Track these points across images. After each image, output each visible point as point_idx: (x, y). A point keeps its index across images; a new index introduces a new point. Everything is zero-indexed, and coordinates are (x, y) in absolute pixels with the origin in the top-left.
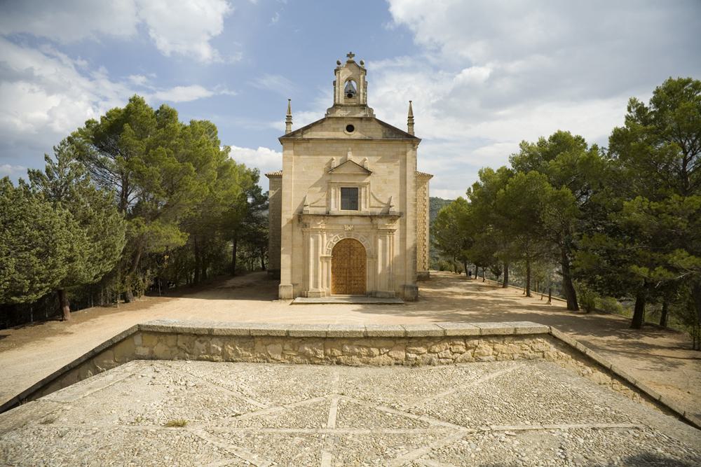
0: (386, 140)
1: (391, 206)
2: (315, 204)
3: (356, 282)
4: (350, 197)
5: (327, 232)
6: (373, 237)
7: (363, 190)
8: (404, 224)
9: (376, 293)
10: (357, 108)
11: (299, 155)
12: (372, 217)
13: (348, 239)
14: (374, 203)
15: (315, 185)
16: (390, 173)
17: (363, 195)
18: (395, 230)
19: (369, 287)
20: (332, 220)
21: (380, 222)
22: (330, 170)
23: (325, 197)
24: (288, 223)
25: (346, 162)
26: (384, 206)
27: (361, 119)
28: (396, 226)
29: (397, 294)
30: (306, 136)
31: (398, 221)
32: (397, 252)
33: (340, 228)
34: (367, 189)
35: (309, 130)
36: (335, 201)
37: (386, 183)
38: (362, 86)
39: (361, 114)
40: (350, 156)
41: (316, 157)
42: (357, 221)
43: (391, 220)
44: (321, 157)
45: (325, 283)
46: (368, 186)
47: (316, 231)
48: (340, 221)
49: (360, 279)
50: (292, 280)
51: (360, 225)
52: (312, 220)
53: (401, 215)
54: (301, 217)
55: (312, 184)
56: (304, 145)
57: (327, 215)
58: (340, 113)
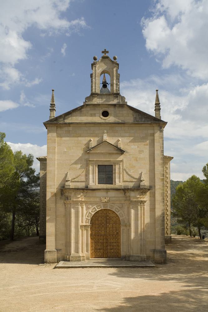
0: (136, 123)
2: (76, 180)
3: (112, 247)
4: (106, 173)
5: (86, 204)
7: (117, 167)
8: (153, 196)
9: (129, 256)
11: (61, 137)
12: (125, 190)
13: (105, 210)
14: (127, 178)
15: (76, 163)
16: (141, 152)
18: (145, 201)
19: (124, 251)
20: (90, 193)
21: (132, 194)
22: (88, 150)
23: (84, 173)
24: (52, 196)
25: (102, 143)
26: (136, 180)
27: (115, 105)
28: (146, 198)
29: (148, 258)
30: (68, 121)
31: (148, 193)
32: (147, 220)
33: (98, 200)
34: (121, 166)
35: (70, 116)
36: (93, 176)
37: (137, 161)
38: (115, 78)
39: (115, 102)
40: (106, 138)
41: (76, 139)
42: (112, 194)
44: (80, 138)
45: (85, 248)
46: (121, 163)
47: (77, 203)
48: (98, 194)
49: (115, 244)
50: (56, 245)
51: (114, 197)
52: (73, 193)
53: (151, 188)
54: (63, 191)
55: (73, 162)
56: (66, 129)
57: (86, 189)
58: (96, 101)
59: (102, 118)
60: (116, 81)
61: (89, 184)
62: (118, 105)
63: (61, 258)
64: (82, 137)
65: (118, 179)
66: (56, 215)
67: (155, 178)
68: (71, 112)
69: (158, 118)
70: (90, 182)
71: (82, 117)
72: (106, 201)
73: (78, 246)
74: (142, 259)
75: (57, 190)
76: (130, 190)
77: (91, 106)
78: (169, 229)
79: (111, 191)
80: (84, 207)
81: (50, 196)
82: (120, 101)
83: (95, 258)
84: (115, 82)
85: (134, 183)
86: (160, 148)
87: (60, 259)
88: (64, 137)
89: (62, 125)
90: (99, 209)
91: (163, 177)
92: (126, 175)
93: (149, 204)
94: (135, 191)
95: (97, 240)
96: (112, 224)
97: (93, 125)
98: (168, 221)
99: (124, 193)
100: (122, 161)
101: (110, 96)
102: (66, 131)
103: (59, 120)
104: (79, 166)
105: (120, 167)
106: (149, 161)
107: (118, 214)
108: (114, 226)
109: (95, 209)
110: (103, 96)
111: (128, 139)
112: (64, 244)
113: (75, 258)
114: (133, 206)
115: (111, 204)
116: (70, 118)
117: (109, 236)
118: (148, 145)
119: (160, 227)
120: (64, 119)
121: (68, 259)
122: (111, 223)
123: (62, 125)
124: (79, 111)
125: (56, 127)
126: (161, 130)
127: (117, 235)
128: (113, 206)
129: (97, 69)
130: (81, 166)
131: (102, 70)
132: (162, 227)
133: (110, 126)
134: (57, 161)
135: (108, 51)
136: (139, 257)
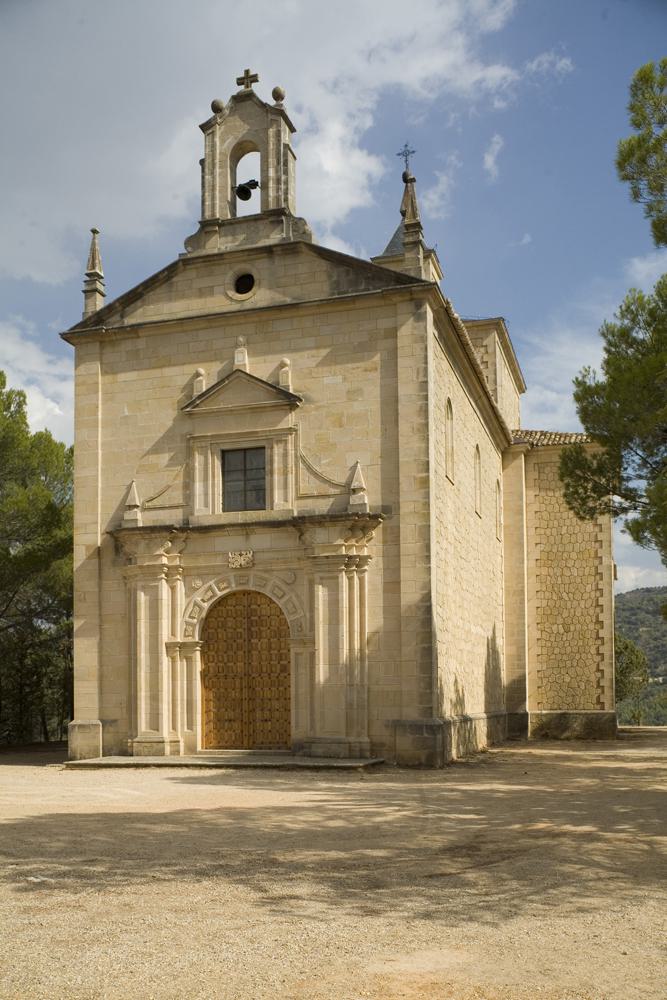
0: (336, 302)
1: (354, 491)
2: (155, 503)
3: (267, 714)
4: (246, 471)
5: (185, 577)
6: (306, 583)
7: (277, 450)
8: (393, 539)
9: (312, 742)
10: (261, 225)
11: (115, 373)
12: (298, 524)
13: (239, 592)
14: (309, 485)
15: (156, 450)
16: (353, 394)
19: (298, 731)
20: (197, 542)
21: (319, 536)
22: (192, 405)
23: (180, 481)
25: (232, 376)
26: (337, 491)
27: (269, 251)
28: (371, 547)
29: (375, 748)
30: (129, 321)
31: (376, 533)
32: (374, 620)
33: (218, 562)
34: (290, 447)
35: (139, 303)
36: (206, 487)
37: (341, 426)
38: (272, 160)
39: (274, 238)
40: (245, 360)
41: (156, 373)
42: (262, 540)
43: (352, 529)
44: (168, 371)
45: (182, 717)
46: (290, 438)
47: (153, 573)
48: (221, 542)
49: (276, 705)
50: (101, 709)
51: (269, 550)
52: (142, 545)
53: (387, 512)
54: (120, 539)
55: (147, 447)
56: (127, 345)
57: (186, 532)
58: (218, 244)
59: (231, 299)
60: (277, 171)
61: (192, 514)
62: (279, 248)
63: (114, 748)
64: (174, 365)
65: (282, 491)
66: (100, 615)
67: (401, 479)
68: (139, 290)
69: (412, 274)
70: (197, 507)
71: (175, 300)
72: (243, 563)
73: (158, 709)
74: (350, 750)
75: (105, 536)
76: (312, 523)
77: (199, 265)
78: (606, 690)
79: (259, 530)
80: (180, 586)
81: (85, 557)
82: (291, 234)
83: (220, 748)
84: (272, 173)
85: (332, 500)
86: (415, 375)
87: (112, 749)
88: (124, 371)
89: (115, 333)
90: (224, 589)
91: (424, 475)
92: (308, 474)
93: (381, 566)
94: (326, 524)
95: (222, 690)
96: (266, 640)
97: (203, 325)
98: (603, 660)
99: (298, 535)
100: (290, 431)
101: (259, 222)
102: (127, 352)
103: (110, 320)
104: (164, 458)
105: (286, 450)
106: (382, 423)
107: (280, 603)
108: (273, 646)
109: (213, 592)
110: (237, 226)
111: (313, 356)
112: (124, 705)
113: (148, 745)
114: (321, 574)
115: (259, 573)
116: (141, 310)
117: (259, 678)
118: (379, 370)
119: (414, 643)
120: (122, 317)
121: (129, 750)
122: (264, 634)
123: (115, 333)
124: (164, 286)
125: (98, 344)
126: (420, 314)
127: (280, 674)
128: (266, 580)
129: (217, 140)
130: (171, 459)
131: (235, 142)
132: (422, 642)
133: (256, 319)
134: (102, 450)
135: (256, 76)
136: (340, 743)
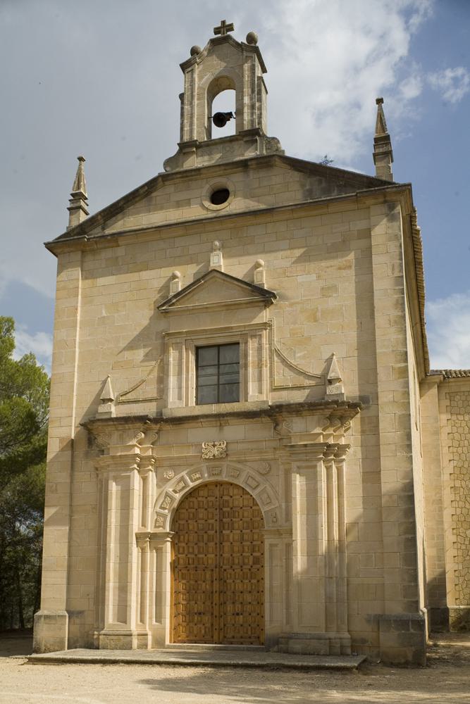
0: (309, 207)
1: (330, 382)
2: (129, 397)
3: (238, 607)
4: (220, 363)
6: (281, 473)
7: (252, 345)
9: (289, 637)
10: (236, 145)
12: (274, 414)
15: (131, 346)
16: (327, 291)
17: (252, 358)
18: (348, 446)
19: (274, 622)
20: (170, 433)
21: (296, 426)
22: (167, 305)
23: (155, 374)
24: (62, 450)
25: (208, 276)
26: (307, 382)
27: (244, 165)
28: (350, 436)
29: (356, 646)
31: (354, 423)
32: (353, 509)
33: (191, 452)
34: (265, 341)
35: (119, 216)
37: (316, 321)
38: (247, 90)
39: (250, 154)
40: (219, 262)
41: (134, 276)
42: (237, 431)
43: (330, 418)
44: (145, 275)
46: (265, 333)
47: (124, 463)
49: (248, 598)
52: (116, 435)
53: (363, 404)
55: (123, 344)
56: (107, 254)
57: (159, 423)
60: (251, 99)
61: (166, 407)
62: (253, 162)
65: (256, 384)
66: (71, 505)
67: (379, 370)
72: (216, 453)
74: (330, 646)
77: (177, 181)
79: (232, 421)
80: (152, 477)
83: (191, 642)
84: (246, 100)
85: (307, 391)
91: (403, 365)
92: (282, 367)
93: (359, 456)
95: (192, 582)
100: (266, 325)
101: (233, 143)
106: (358, 318)
107: (254, 494)
108: (246, 537)
109: (185, 482)
114: (299, 464)
117: (231, 571)
118: (353, 268)
120: (103, 229)
121: (95, 643)
122: (236, 526)
123: (96, 242)
124: (144, 200)
125: (80, 253)
129: (196, 76)
130: (146, 355)
132: (406, 533)
134: (79, 348)
135: (231, 25)
136: (320, 639)
